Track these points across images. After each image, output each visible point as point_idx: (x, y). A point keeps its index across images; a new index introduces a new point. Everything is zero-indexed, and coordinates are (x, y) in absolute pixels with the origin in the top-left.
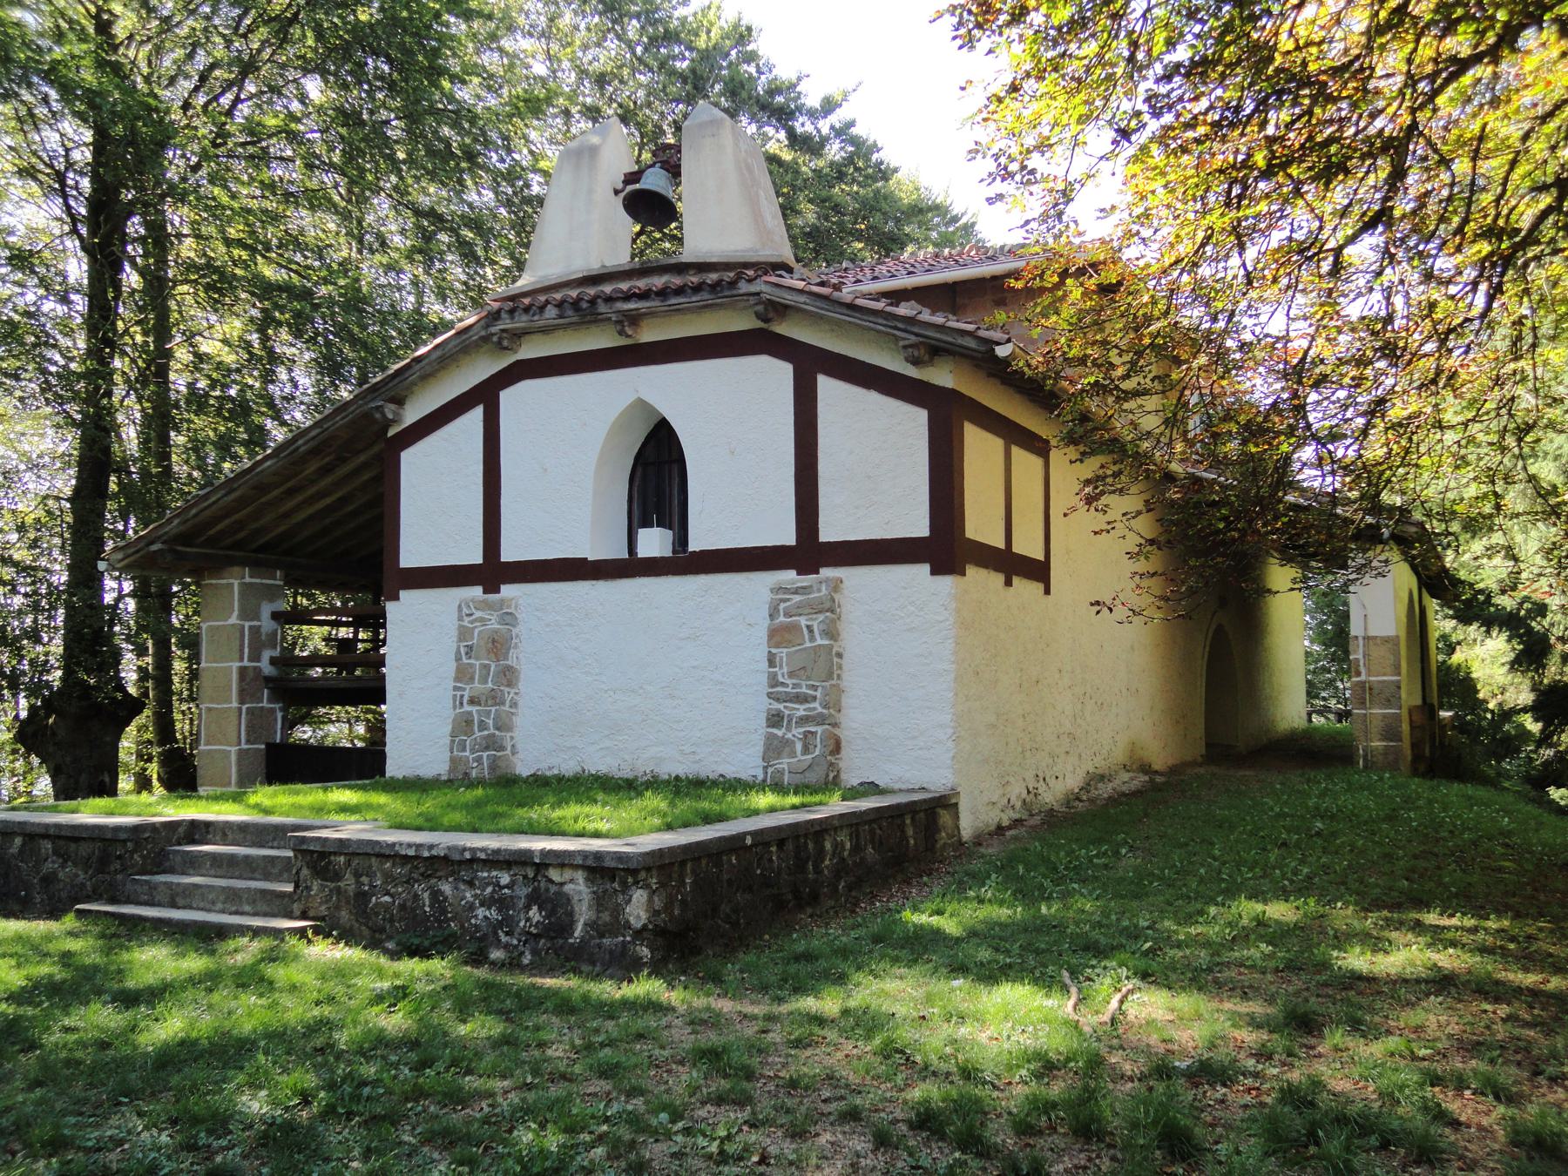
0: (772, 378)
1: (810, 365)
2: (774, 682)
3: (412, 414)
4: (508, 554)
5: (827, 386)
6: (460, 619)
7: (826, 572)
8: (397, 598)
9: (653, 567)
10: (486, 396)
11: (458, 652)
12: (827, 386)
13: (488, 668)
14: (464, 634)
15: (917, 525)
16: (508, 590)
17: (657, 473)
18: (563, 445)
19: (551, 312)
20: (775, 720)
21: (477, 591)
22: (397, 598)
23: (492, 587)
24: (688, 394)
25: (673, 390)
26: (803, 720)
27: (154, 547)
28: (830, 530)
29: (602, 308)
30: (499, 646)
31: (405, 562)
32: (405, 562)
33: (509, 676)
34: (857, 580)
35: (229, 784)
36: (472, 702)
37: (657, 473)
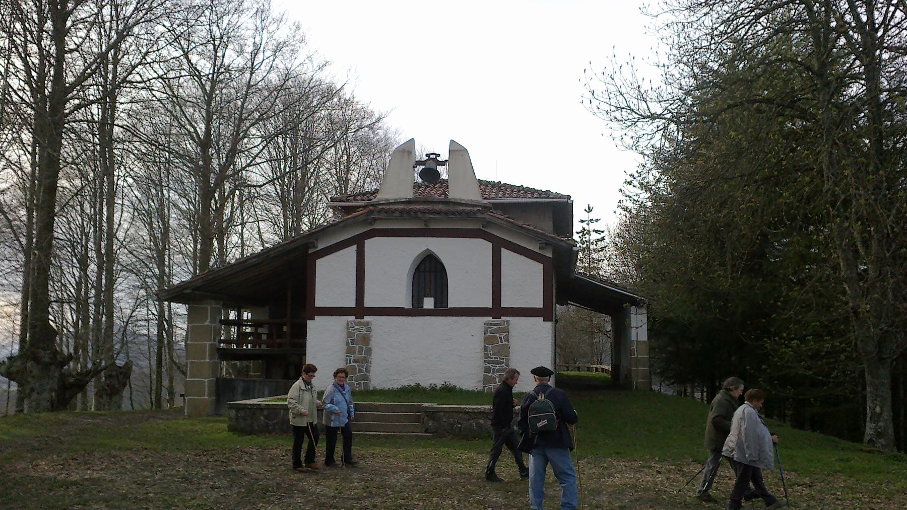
0: (484, 248)
1: (498, 245)
2: (486, 356)
3: (321, 246)
4: (367, 304)
5: (504, 252)
6: (348, 328)
7: (504, 318)
8: (313, 319)
9: (429, 313)
10: (359, 242)
11: (347, 342)
12: (504, 252)
13: (359, 347)
14: (350, 335)
15: (489, 304)
16: (367, 318)
17: (430, 276)
18: (391, 264)
19: (397, 214)
20: (487, 370)
21: (353, 318)
22: (313, 319)
23: (359, 316)
24: (447, 250)
25: (441, 247)
26: (498, 371)
27: (188, 291)
28: (505, 303)
29: (419, 214)
30: (366, 340)
31: (318, 304)
32: (318, 304)
33: (369, 351)
34: (514, 321)
35: (204, 395)
36: (355, 361)
37: (430, 276)
